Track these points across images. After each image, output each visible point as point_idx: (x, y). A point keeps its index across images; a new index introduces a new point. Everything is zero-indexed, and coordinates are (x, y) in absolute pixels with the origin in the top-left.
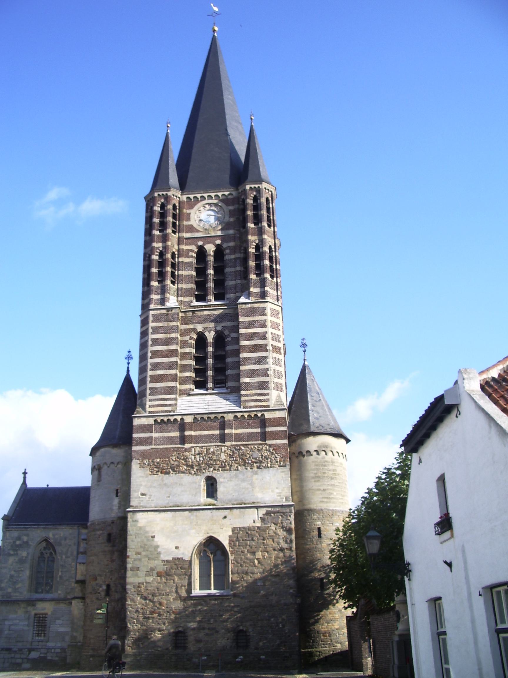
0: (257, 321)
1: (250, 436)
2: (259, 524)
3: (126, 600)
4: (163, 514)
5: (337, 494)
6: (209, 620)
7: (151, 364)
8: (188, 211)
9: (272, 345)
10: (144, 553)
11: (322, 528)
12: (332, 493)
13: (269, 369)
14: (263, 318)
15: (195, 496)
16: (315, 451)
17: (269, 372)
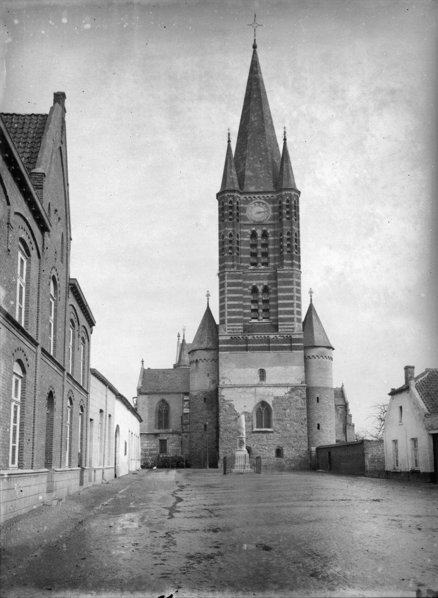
8: (246, 206)
14: (291, 279)
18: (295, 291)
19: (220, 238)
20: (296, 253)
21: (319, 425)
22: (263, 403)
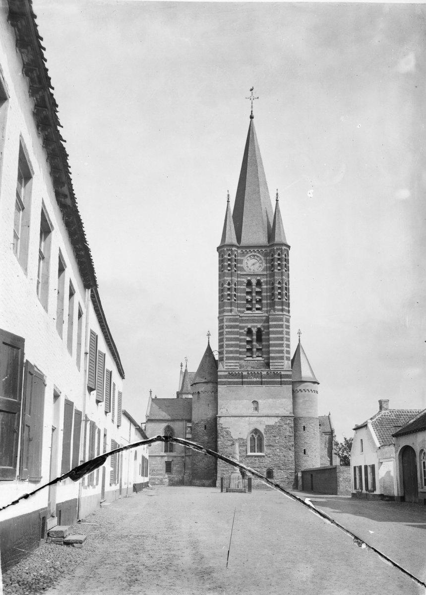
8: (242, 258)
18: (284, 333)
19: (219, 286)
20: (286, 300)
22: (256, 431)
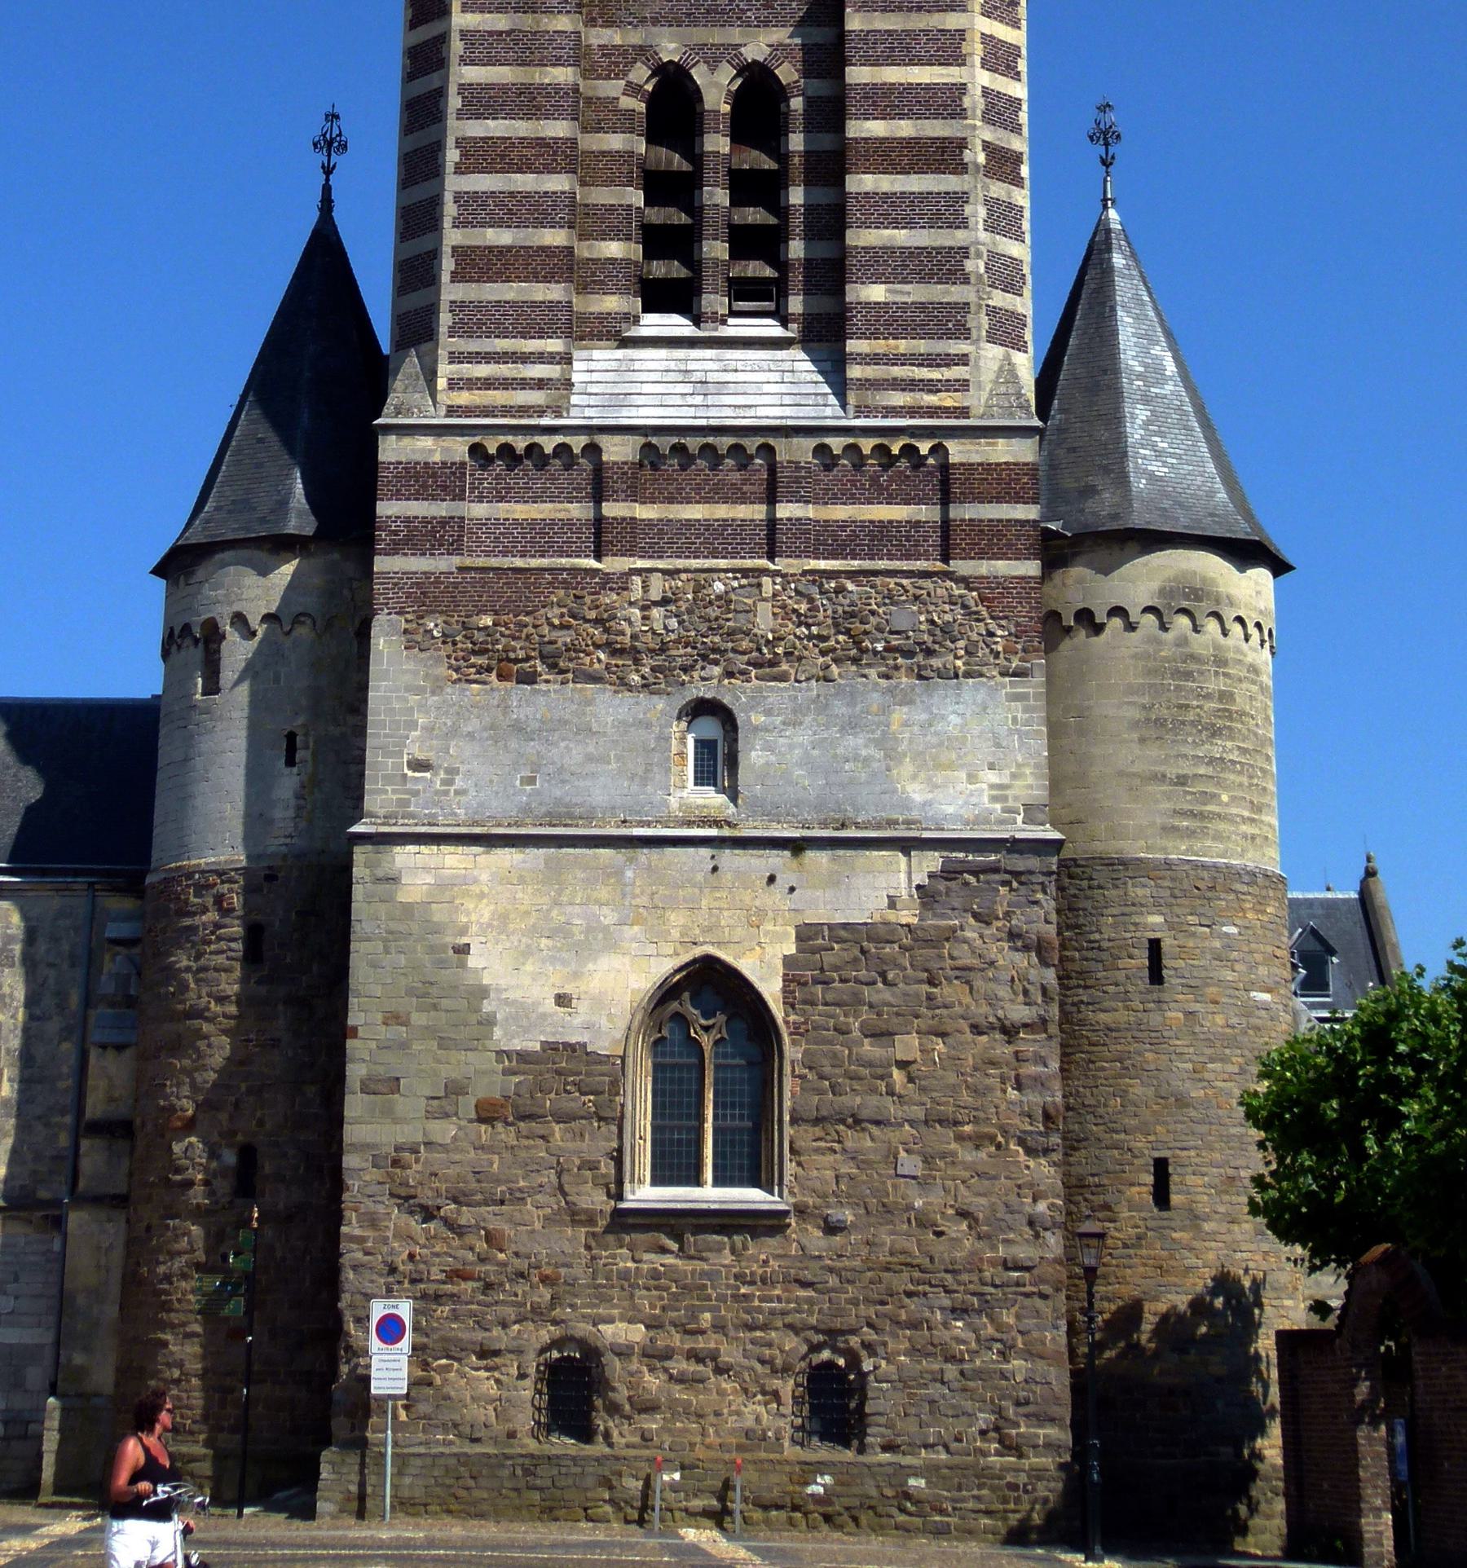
0: (926, 32)
1: (880, 537)
2: (908, 916)
3: (337, 1218)
4: (507, 857)
5: (1233, 798)
6: (695, 1318)
7: (458, 197)
9: (987, 146)
10: (419, 1019)
11: (1167, 944)
12: (1214, 796)
13: (972, 250)
15: (644, 781)
16: (1149, 609)
17: (969, 265)
21: (1161, 1168)
